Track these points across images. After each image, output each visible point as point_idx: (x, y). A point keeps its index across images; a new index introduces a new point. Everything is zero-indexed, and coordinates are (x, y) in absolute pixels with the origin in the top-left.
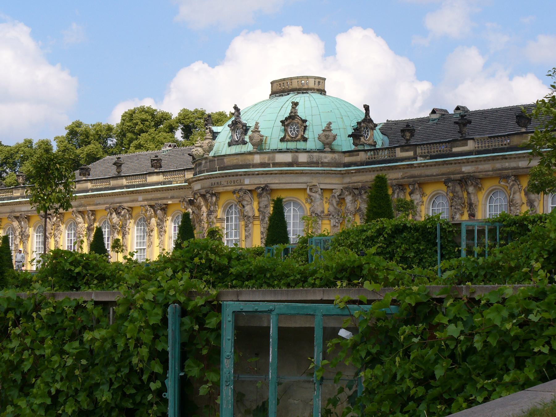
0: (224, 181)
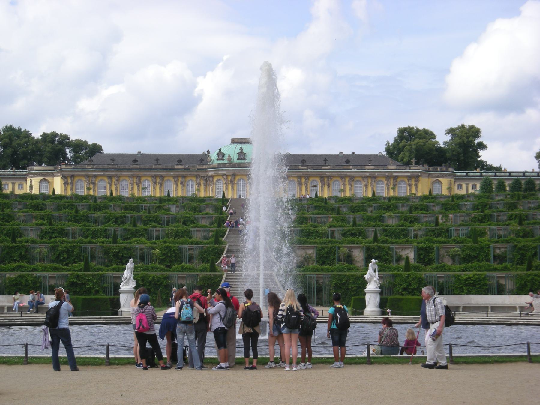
0: (241, 172)
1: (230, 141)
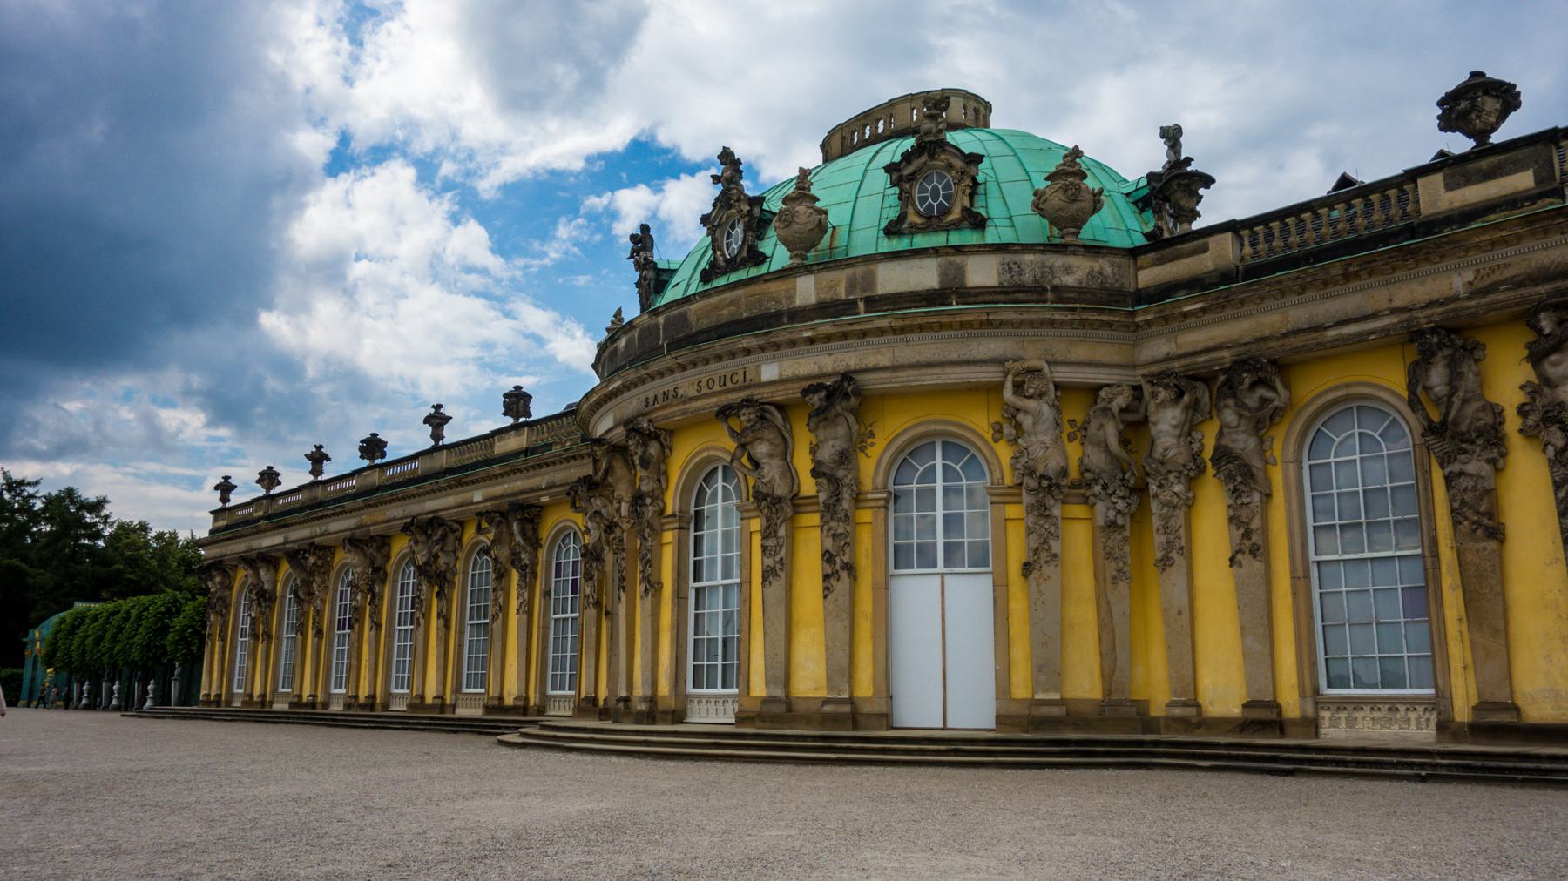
0: (686, 383)
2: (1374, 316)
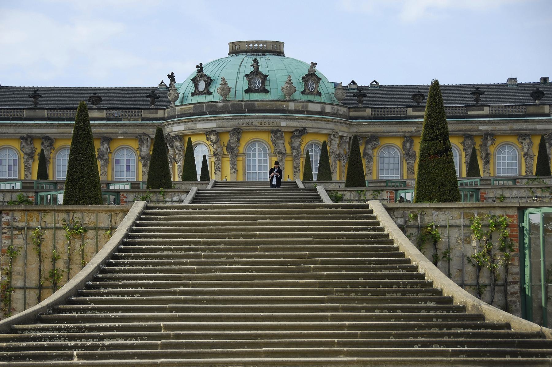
0: (256, 122)
1: (227, 50)
2: (399, 132)
